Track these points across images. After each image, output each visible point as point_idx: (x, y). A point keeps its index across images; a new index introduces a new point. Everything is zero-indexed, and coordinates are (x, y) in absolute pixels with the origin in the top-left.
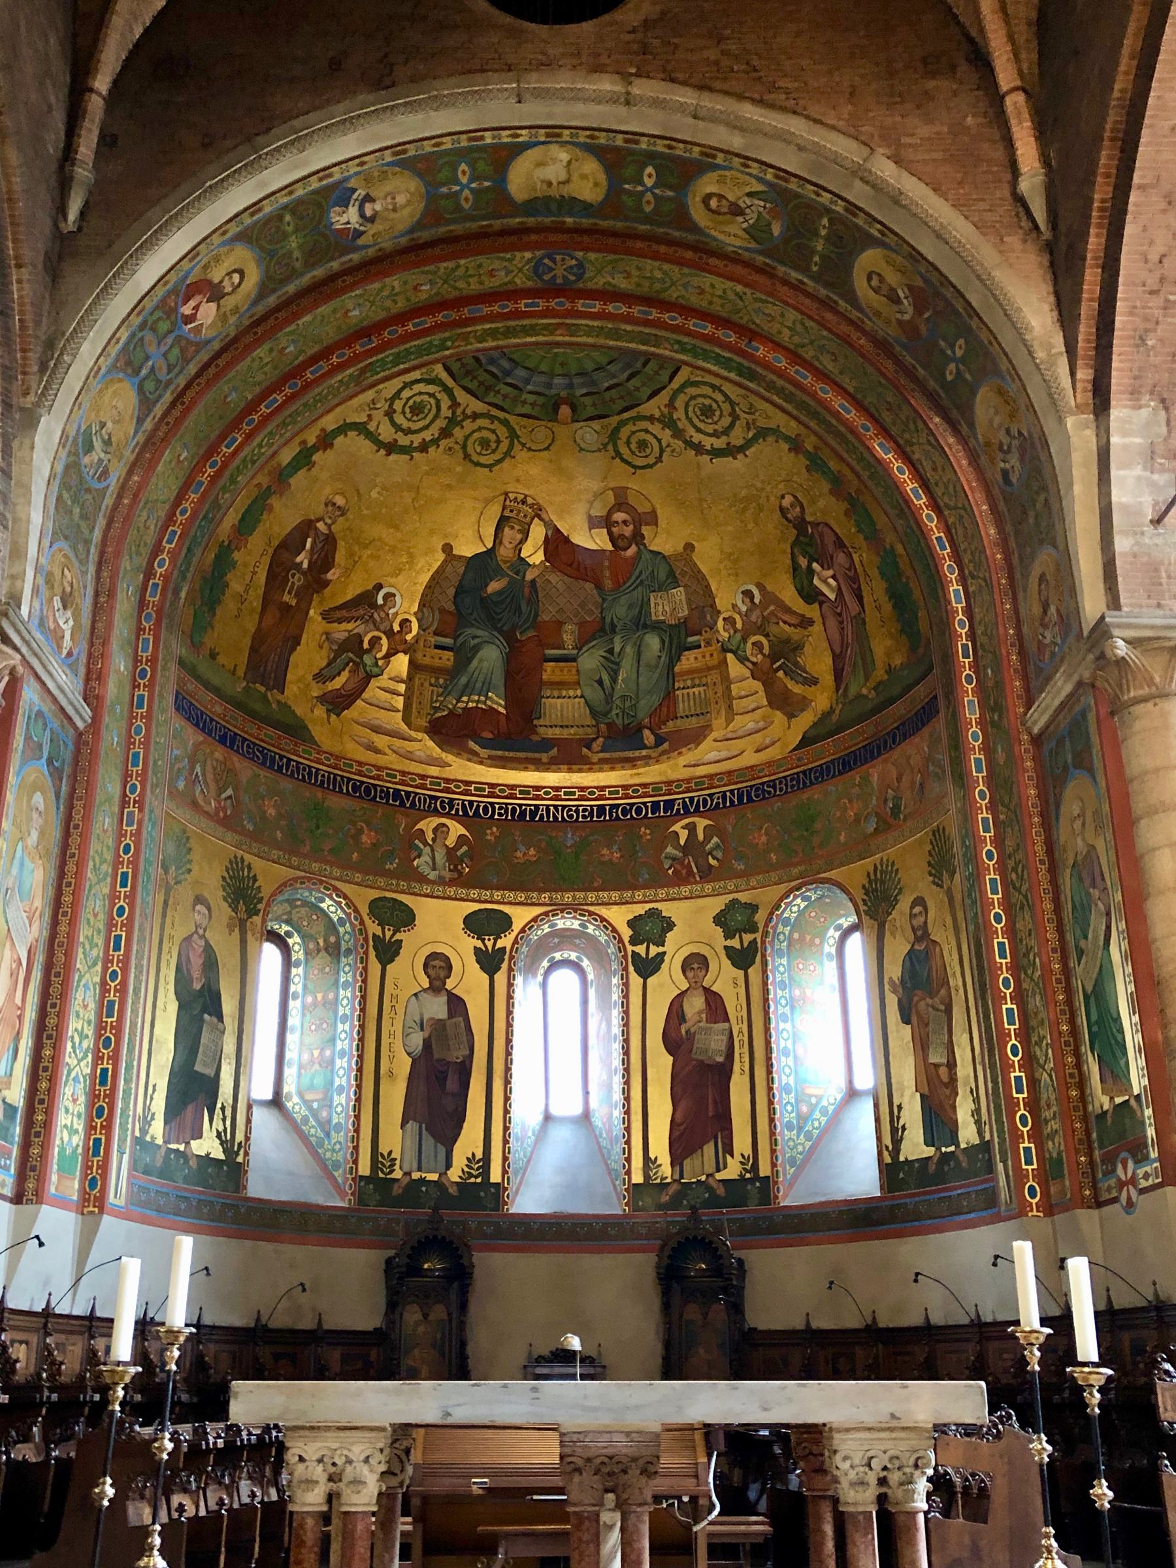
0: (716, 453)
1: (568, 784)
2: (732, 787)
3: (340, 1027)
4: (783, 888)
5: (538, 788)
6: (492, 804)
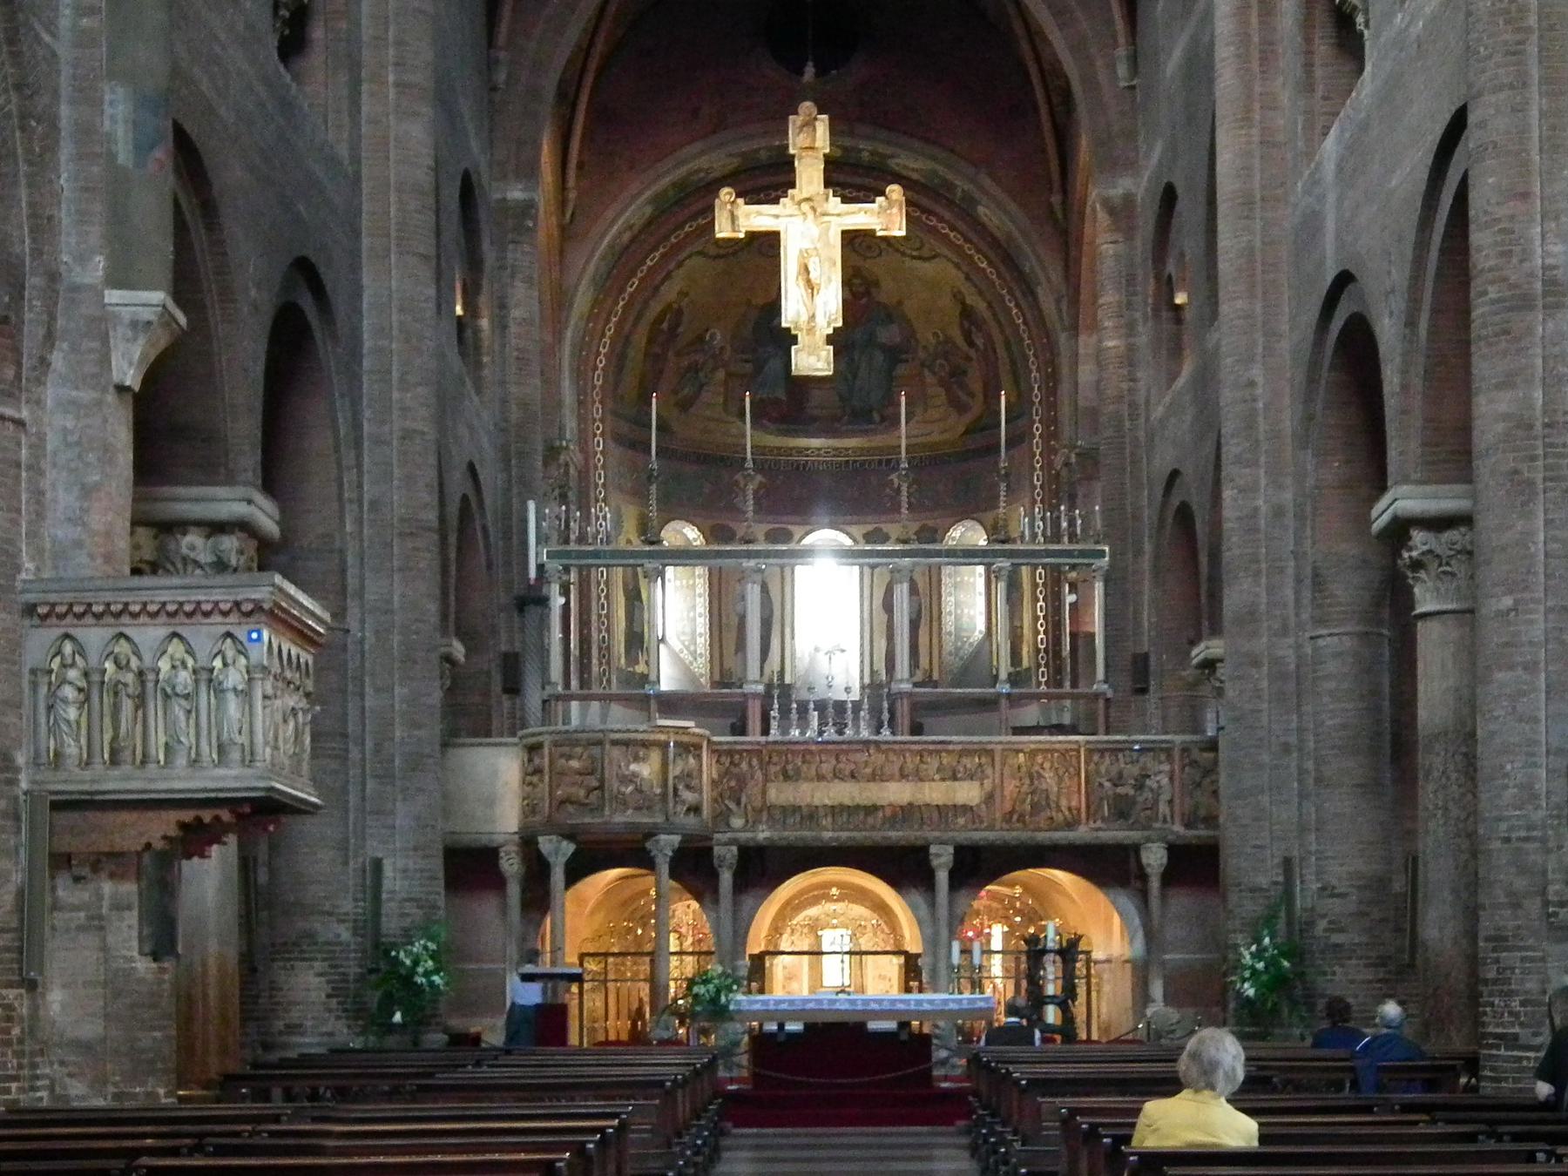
3: (698, 599)
4: (952, 520)
5: (807, 449)
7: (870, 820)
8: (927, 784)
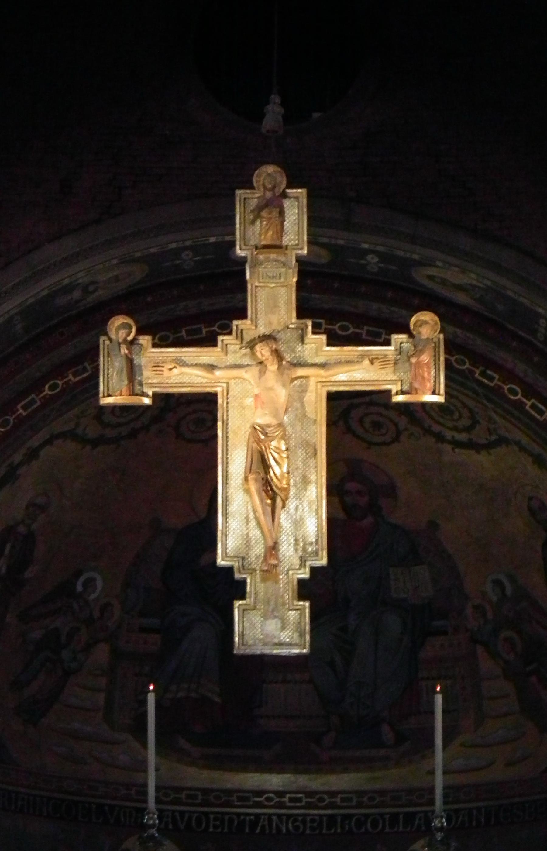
0: (457, 444)
1: (294, 787)
2: (480, 804)
5: (260, 793)
6: (206, 814)
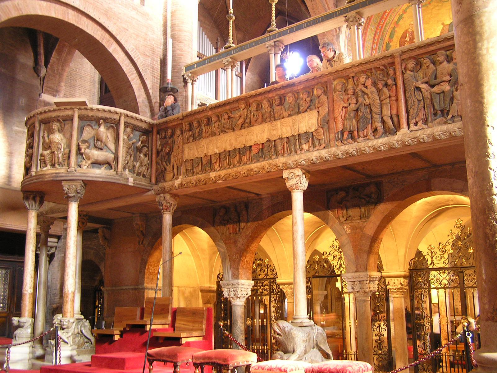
7: (244, 159)
8: (278, 122)
